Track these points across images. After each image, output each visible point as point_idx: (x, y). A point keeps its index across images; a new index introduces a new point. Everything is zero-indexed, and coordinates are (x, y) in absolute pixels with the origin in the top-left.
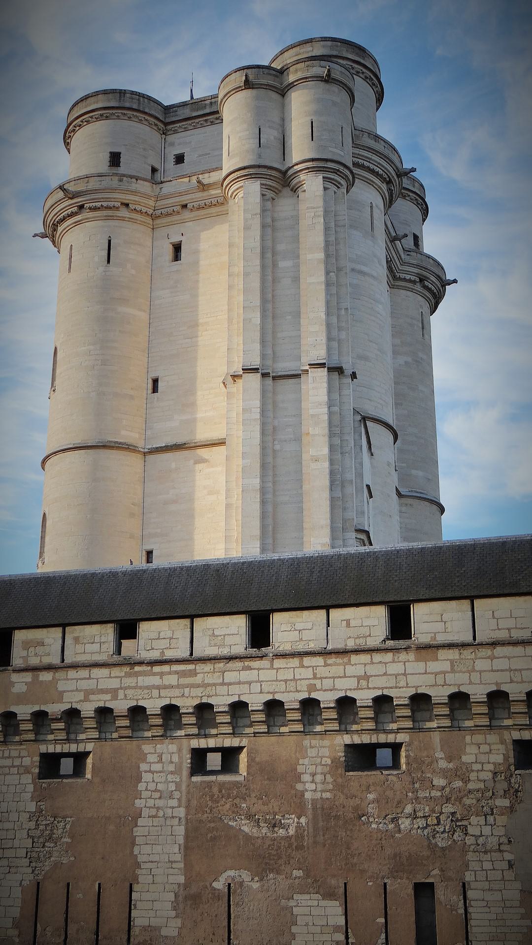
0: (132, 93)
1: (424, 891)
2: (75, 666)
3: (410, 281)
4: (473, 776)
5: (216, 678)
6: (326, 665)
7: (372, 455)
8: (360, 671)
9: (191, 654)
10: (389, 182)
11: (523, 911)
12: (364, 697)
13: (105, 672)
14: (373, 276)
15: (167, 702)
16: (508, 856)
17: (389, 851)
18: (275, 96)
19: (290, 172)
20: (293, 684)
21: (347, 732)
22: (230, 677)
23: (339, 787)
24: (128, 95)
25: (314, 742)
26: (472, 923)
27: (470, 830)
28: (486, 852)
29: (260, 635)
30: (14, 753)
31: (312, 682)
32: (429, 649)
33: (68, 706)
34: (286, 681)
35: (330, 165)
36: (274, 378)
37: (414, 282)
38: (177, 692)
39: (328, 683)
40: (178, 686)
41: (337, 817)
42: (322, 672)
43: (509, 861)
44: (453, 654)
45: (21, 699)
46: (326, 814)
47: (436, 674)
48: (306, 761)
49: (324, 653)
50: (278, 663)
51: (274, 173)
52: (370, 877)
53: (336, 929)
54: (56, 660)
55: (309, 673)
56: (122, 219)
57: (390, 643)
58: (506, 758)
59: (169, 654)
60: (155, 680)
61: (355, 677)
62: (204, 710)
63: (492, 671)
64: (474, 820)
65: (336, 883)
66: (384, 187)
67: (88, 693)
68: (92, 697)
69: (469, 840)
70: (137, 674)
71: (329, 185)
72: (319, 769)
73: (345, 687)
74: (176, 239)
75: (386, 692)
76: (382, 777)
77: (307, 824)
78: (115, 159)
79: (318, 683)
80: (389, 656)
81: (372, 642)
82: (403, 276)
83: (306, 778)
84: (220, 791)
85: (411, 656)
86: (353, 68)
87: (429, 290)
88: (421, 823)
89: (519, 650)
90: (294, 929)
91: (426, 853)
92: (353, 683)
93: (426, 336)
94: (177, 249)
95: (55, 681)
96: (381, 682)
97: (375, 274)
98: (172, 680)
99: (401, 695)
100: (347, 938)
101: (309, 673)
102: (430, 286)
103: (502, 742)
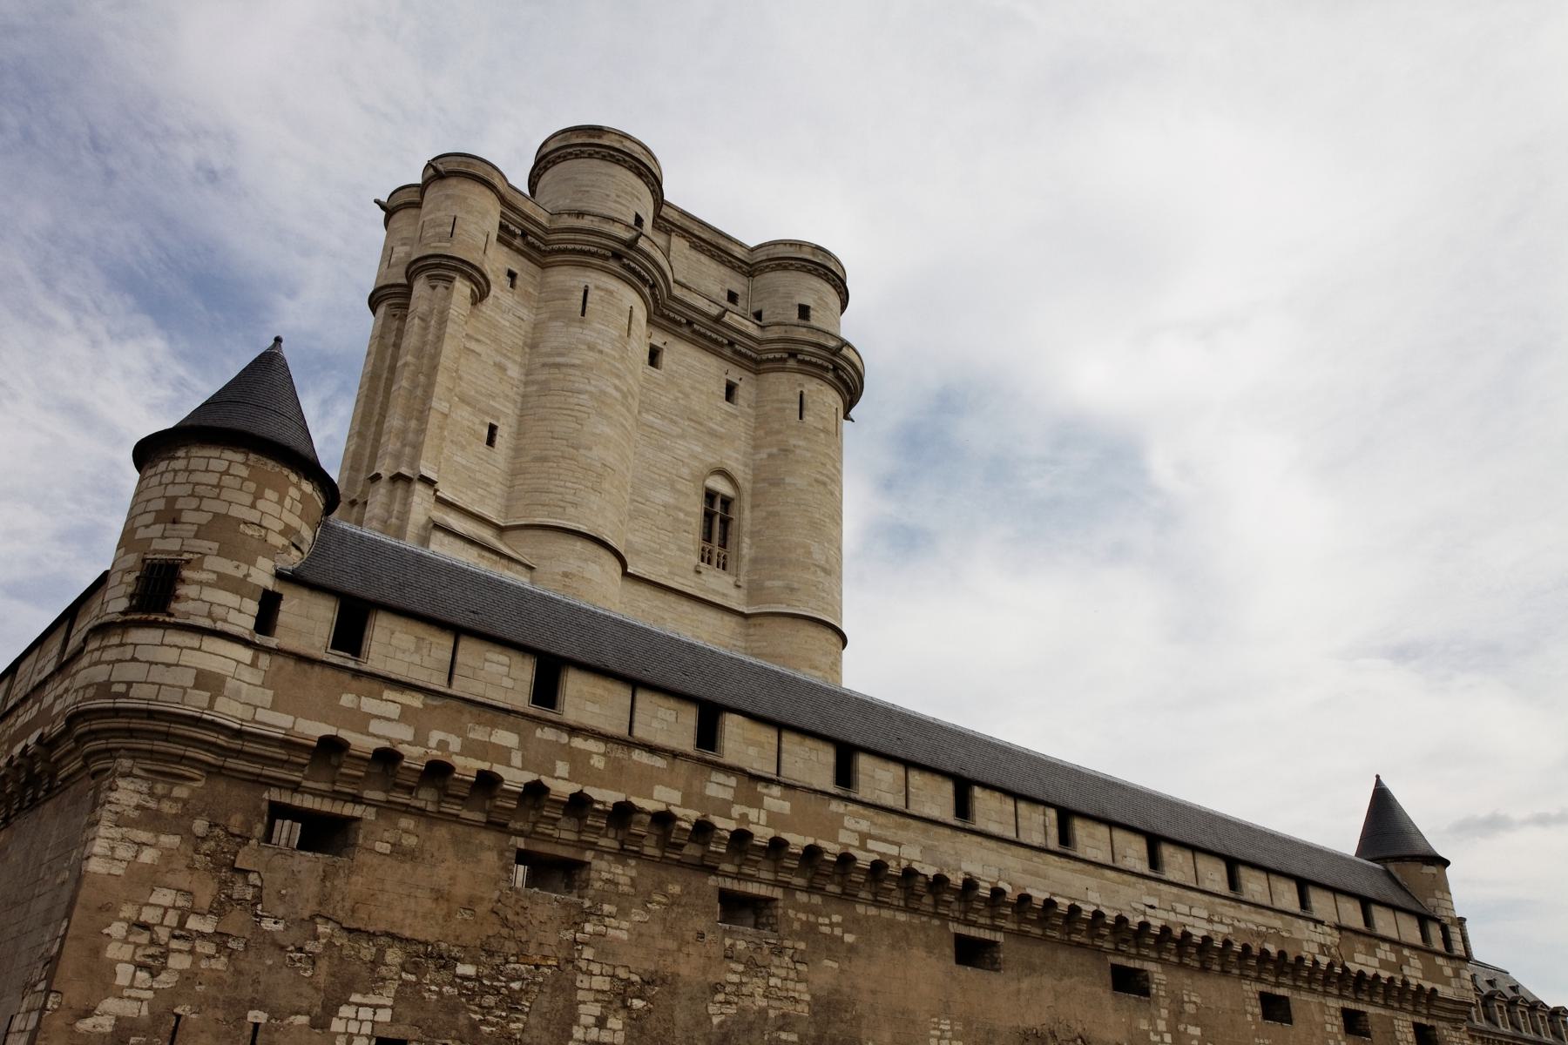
3: (774, 360)
10: (617, 256)
51: (398, 290)
66: (613, 265)
82: (764, 357)
97: (577, 362)
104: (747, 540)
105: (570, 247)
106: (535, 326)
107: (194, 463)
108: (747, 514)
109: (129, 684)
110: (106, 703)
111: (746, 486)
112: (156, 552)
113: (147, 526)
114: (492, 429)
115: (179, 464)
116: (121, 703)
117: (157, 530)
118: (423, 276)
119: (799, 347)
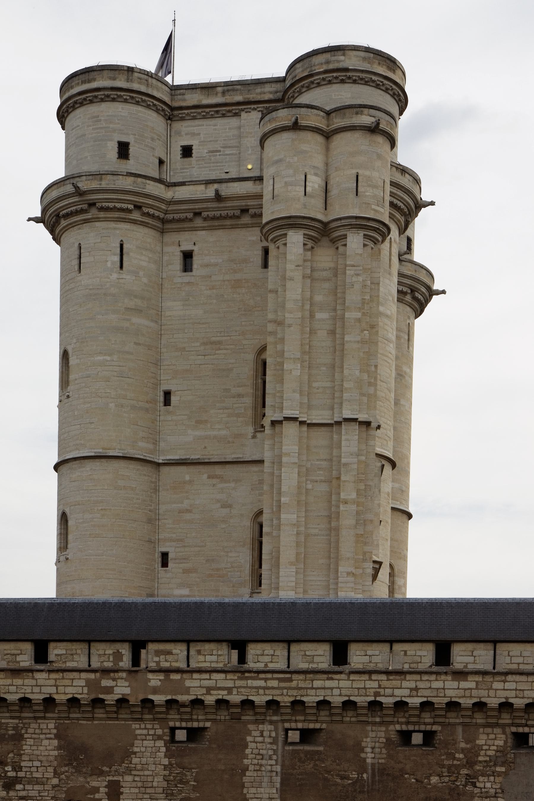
2: (200, 671)
5: (308, 684)
6: (388, 680)
8: (412, 685)
13: (222, 676)
15: (270, 698)
20: (364, 691)
21: (398, 723)
22: (317, 684)
25: (374, 728)
29: (340, 656)
30: (149, 726)
31: (378, 690)
33: (194, 697)
34: (358, 689)
38: (278, 692)
39: (388, 691)
40: (278, 688)
42: (385, 684)
45: (155, 691)
48: (368, 740)
49: (387, 673)
50: (352, 677)
54: (183, 665)
55: (375, 685)
59: (271, 666)
60: (262, 683)
61: (408, 688)
62: (297, 704)
67: (209, 690)
68: (212, 692)
70: (247, 678)
73: (401, 694)
75: (430, 699)
79: (382, 691)
80: (433, 677)
88: (447, 779)
92: (407, 692)
95: (182, 680)
96: (427, 693)
98: (275, 683)
99: (440, 701)
101: (375, 685)
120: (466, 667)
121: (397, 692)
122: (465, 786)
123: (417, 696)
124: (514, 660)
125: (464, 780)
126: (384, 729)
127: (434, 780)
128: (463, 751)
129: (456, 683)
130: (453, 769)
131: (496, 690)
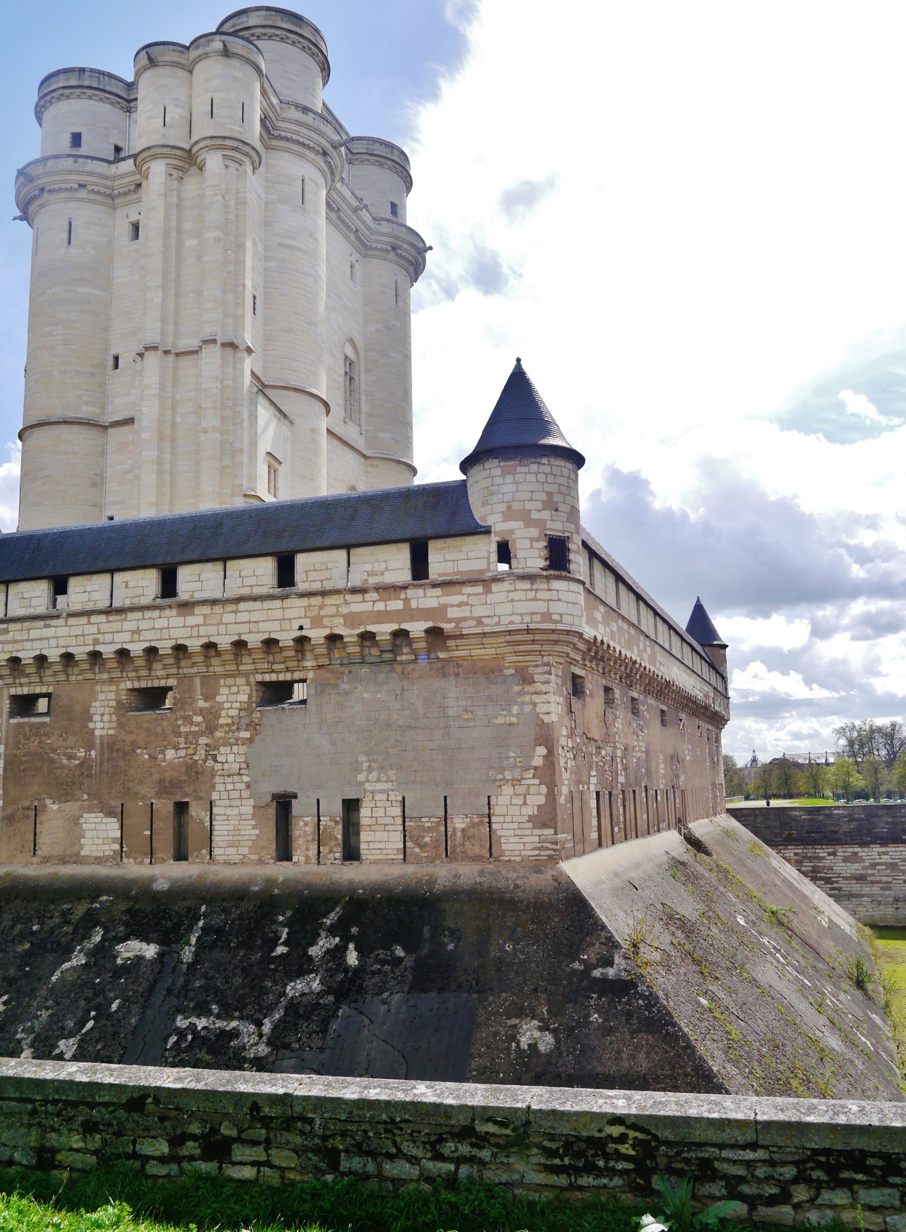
0: (92, 70)
1: (181, 808)
3: (382, 250)
4: (223, 713)
6: (108, 622)
7: (292, 423)
8: (133, 626)
9: (6, 615)
10: (325, 154)
11: (254, 822)
12: (137, 649)
14: (301, 250)
16: (246, 779)
17: (156, 777)
18: (181, 73)
19: (194, 150)
21: (129, 678)
22: (34, 634)
23: (120, 725)
24: (87, 74)
25: (105, 688)
26: (215, 833)
27: (219, 758)
28: (229, 776)
31: (97, 636)
32: (187, 607)
34: (76, 636)
35: (228, 142)
36: (177, 355)
37: (387, 251)
39: (108, 637)
41: (118, 750)
42: (105, 627)
43: (246, 783)
44: (206, 610)
46: (111, 746)
47: (192, 627)
48: (97, 704)
49: (109, 611)
50: (71, 621)
51: (178, 153)
52: (141, 799)
53: (114, 840)
55: (93, 629)
56: (82, 200)
57: (159, 601)
58: (250, 696)
63: (236, 623)
64: (223, 749)
65: (116, 803)
66: (320, 160)
69: (218, 767)
71: (228, 162)
72: (107, 710)
73: (123, 640)
74: (134, 218)
76: (154, 716)
77: (96, 756)
78: (76, 139)
79: (100, 637)
80: (156, 613)
81: (146, 600)
82: (374, 245)
83: (97, 718)
84: (31, 730)
85: (174, 612)
86: (288, 38)
87: (404, 258)
88: (183, 753)
89: (258, 605)
90: (83, 841)
91: (184, 778)
92: (127, 636)
93: (400, 303)
94: (136, 227)
100: (122, 847)
102: (404, 254)
103: (248, 684)
104: (363, 397)
105: (295, 137)
106: (267, 204)
107: (556, 470)
108: (363, 377)
109: (561, 615)
110: (552, 626)
111: (362, 353)
112: (551, 529)
113: (539, 511)
114: (255, 298)
115: (547, 469)
116: (560, 627)
117: (546, 515)
118: (220, 153)
119: (400, 243)
120: (192, 596)
121: (119, 637)
122: (205, 761)
123: (140, 641)
124: (247, 582)
125: (203, 752)
126: (114, 688)
127: (170, 754)
128: (201, 712)
129: (182, 619)
130: (190, 737)
131: (227, 624)
